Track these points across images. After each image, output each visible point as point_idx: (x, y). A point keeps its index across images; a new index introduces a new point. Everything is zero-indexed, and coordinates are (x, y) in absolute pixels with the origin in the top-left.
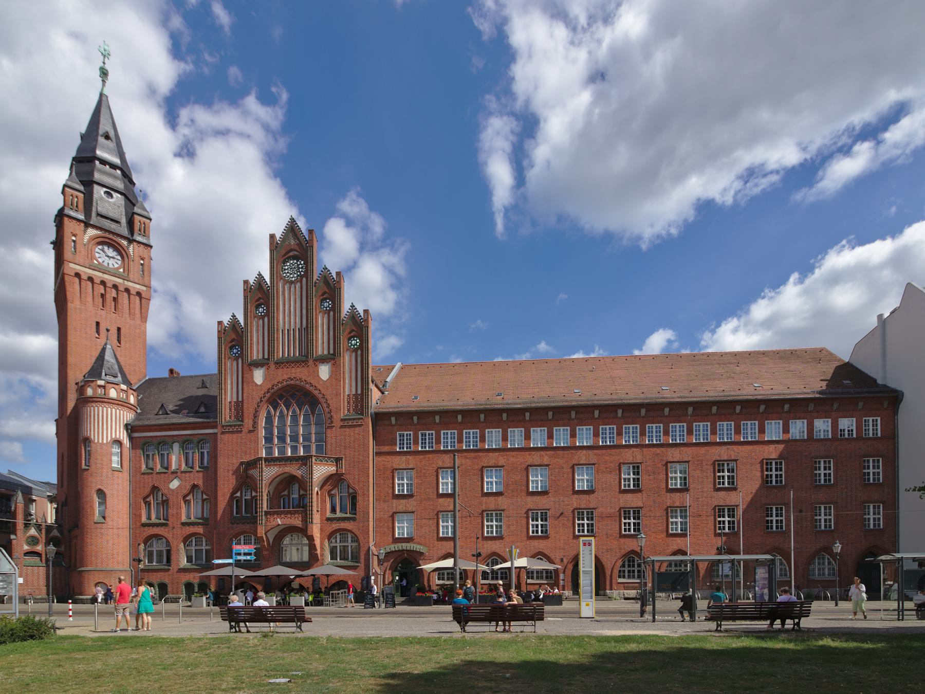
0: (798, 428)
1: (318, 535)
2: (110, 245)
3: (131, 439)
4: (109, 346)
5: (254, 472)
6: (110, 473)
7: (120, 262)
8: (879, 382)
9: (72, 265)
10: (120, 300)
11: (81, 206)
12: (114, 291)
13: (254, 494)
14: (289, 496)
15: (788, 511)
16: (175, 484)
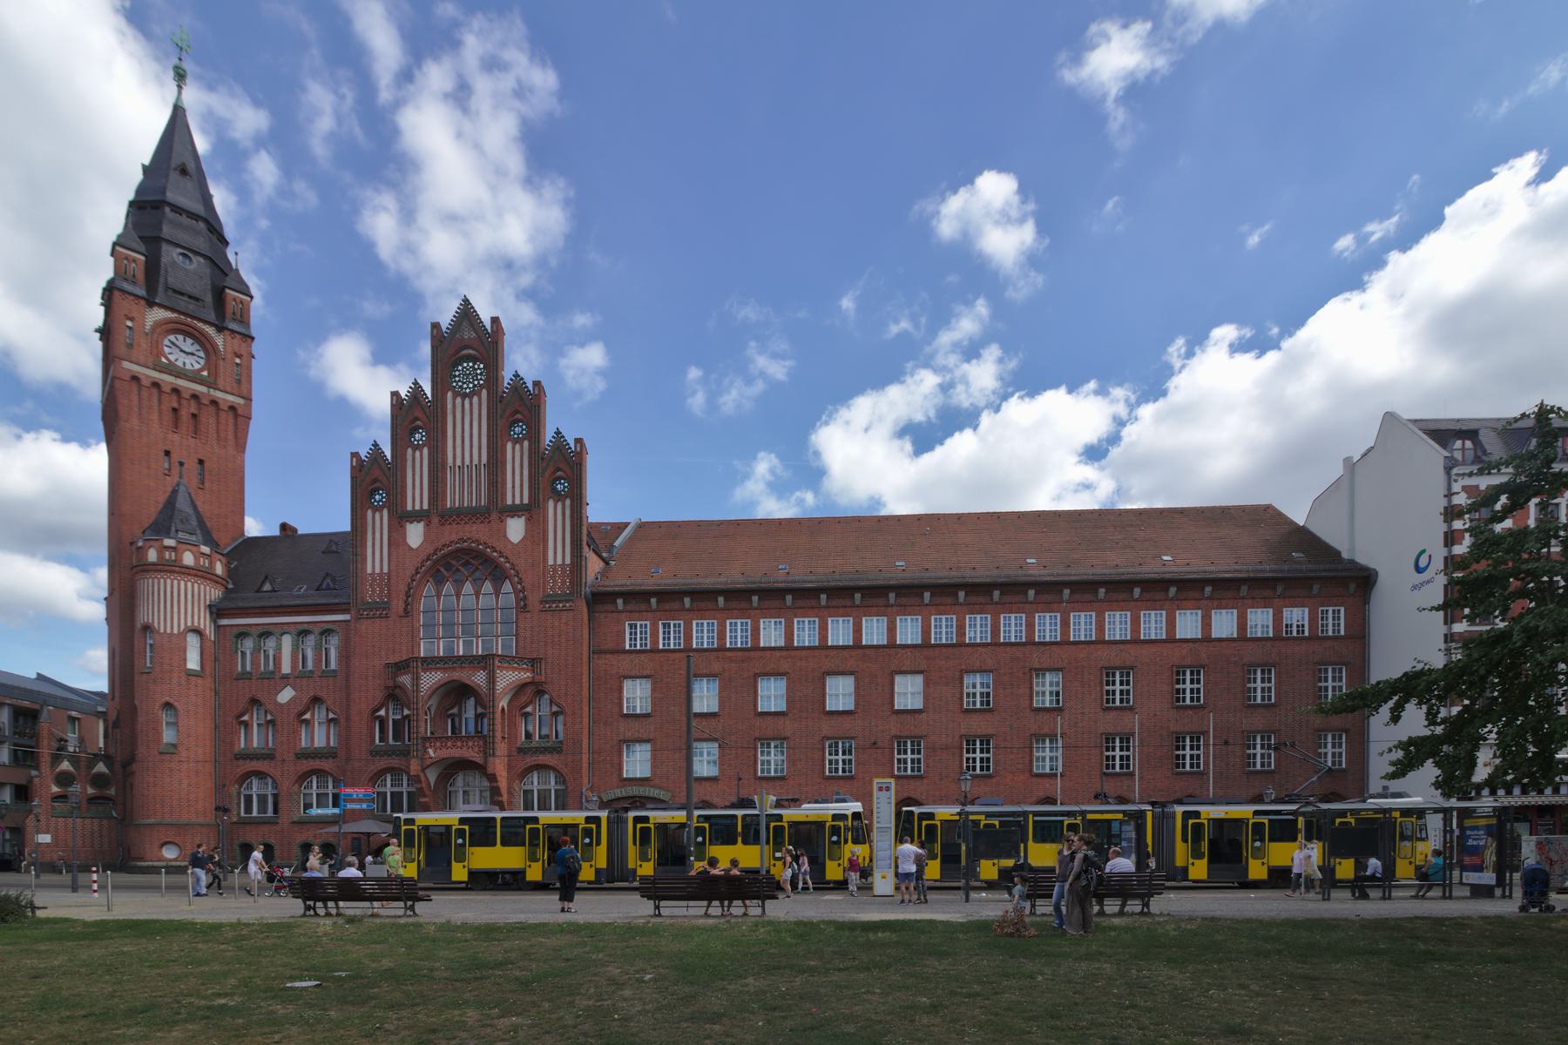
0: (1224, 624)
1: (504, 774)
2: (187, 334)
3: (218, 628)
4: (182, 488)
5: (405, 680)
6: (184, 679)
7: (202, 362)
8: (1345, 555)
9: (126, 365)
10: (203, 419)
11: (141, 276)
12: (193, 403)
13: (406, 712)
14: (460, 715)
15: (1207, 745)
16: (286, 695)
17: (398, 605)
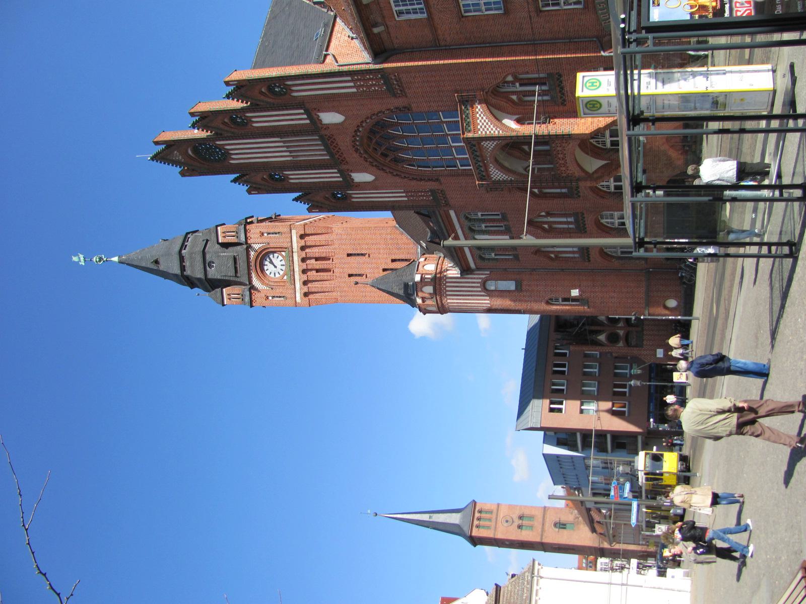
3: (478, 269)
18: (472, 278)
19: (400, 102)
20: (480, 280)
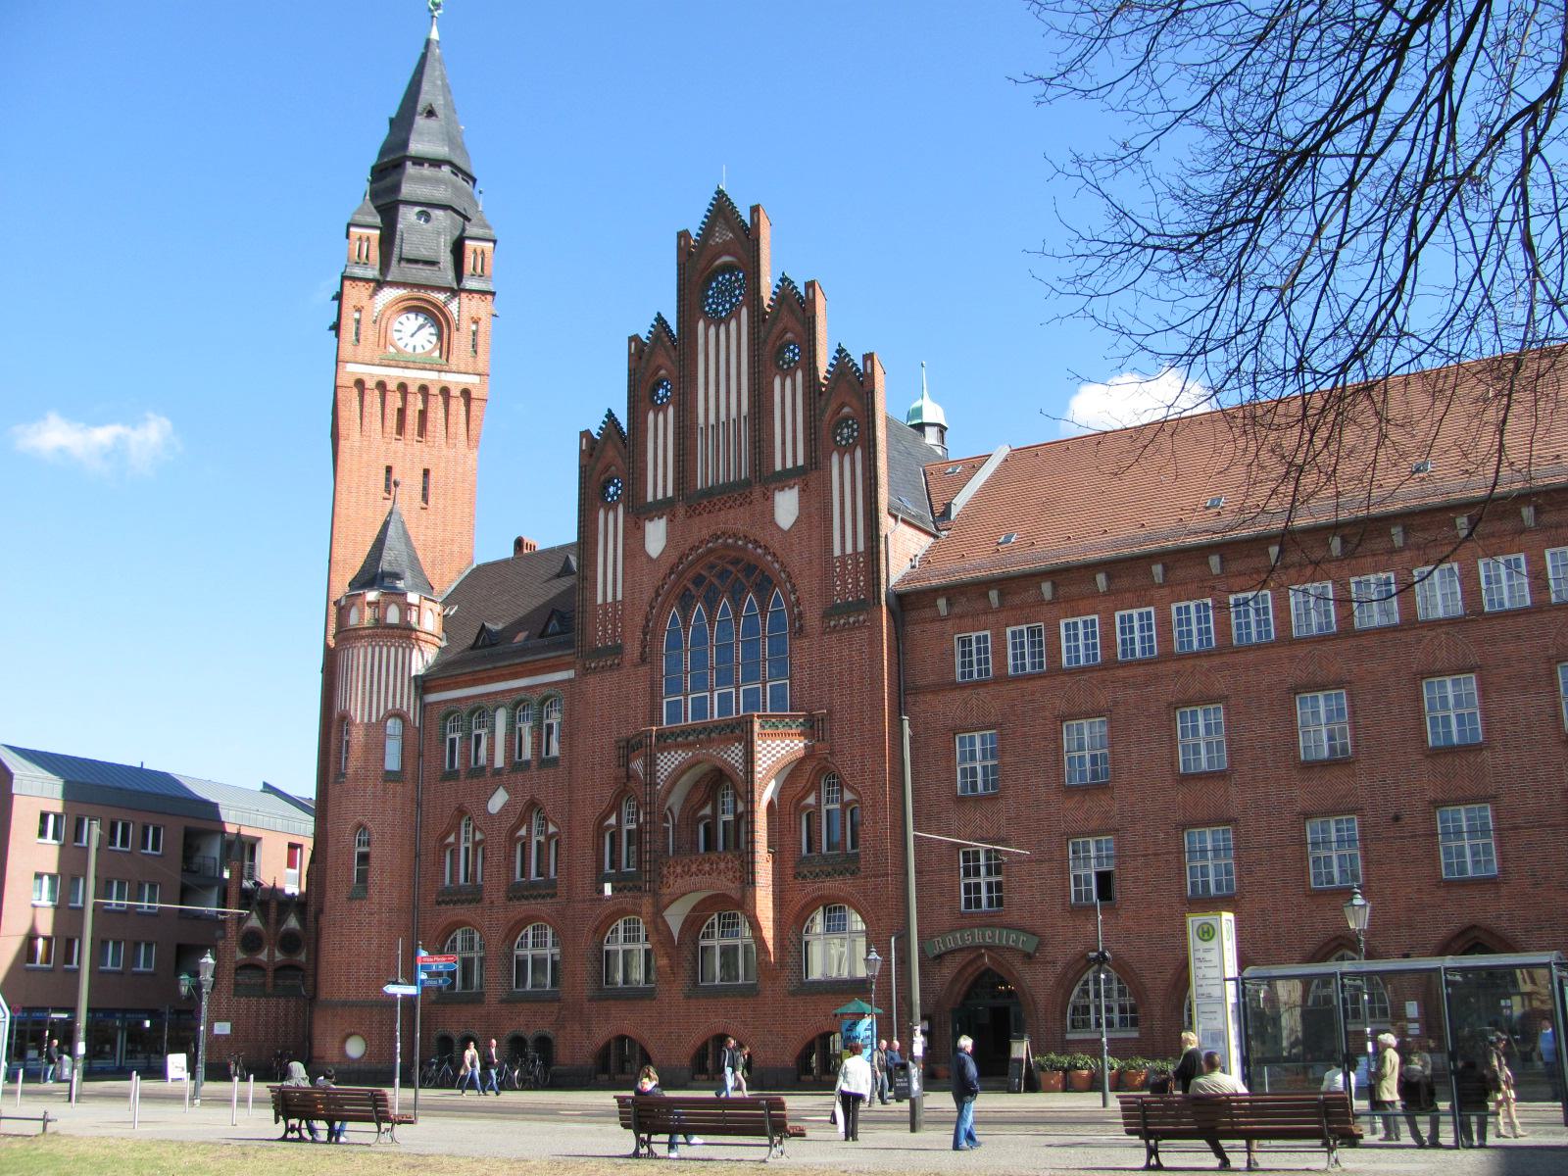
3: (424, 707)
14: (715, 816)
16: (498, 801)
17: (633, 649)
18: (409, 694)
19: (813, 620)
20: (405, 709)
